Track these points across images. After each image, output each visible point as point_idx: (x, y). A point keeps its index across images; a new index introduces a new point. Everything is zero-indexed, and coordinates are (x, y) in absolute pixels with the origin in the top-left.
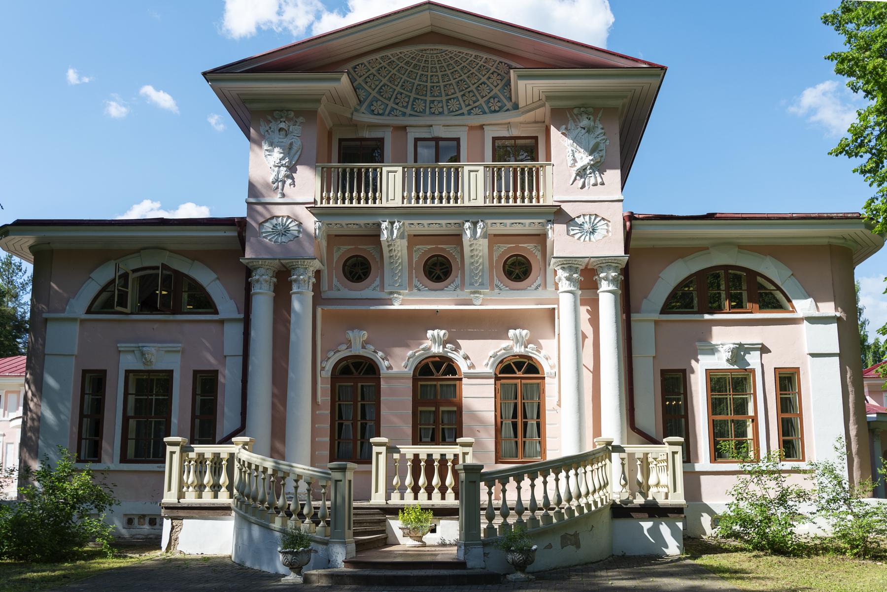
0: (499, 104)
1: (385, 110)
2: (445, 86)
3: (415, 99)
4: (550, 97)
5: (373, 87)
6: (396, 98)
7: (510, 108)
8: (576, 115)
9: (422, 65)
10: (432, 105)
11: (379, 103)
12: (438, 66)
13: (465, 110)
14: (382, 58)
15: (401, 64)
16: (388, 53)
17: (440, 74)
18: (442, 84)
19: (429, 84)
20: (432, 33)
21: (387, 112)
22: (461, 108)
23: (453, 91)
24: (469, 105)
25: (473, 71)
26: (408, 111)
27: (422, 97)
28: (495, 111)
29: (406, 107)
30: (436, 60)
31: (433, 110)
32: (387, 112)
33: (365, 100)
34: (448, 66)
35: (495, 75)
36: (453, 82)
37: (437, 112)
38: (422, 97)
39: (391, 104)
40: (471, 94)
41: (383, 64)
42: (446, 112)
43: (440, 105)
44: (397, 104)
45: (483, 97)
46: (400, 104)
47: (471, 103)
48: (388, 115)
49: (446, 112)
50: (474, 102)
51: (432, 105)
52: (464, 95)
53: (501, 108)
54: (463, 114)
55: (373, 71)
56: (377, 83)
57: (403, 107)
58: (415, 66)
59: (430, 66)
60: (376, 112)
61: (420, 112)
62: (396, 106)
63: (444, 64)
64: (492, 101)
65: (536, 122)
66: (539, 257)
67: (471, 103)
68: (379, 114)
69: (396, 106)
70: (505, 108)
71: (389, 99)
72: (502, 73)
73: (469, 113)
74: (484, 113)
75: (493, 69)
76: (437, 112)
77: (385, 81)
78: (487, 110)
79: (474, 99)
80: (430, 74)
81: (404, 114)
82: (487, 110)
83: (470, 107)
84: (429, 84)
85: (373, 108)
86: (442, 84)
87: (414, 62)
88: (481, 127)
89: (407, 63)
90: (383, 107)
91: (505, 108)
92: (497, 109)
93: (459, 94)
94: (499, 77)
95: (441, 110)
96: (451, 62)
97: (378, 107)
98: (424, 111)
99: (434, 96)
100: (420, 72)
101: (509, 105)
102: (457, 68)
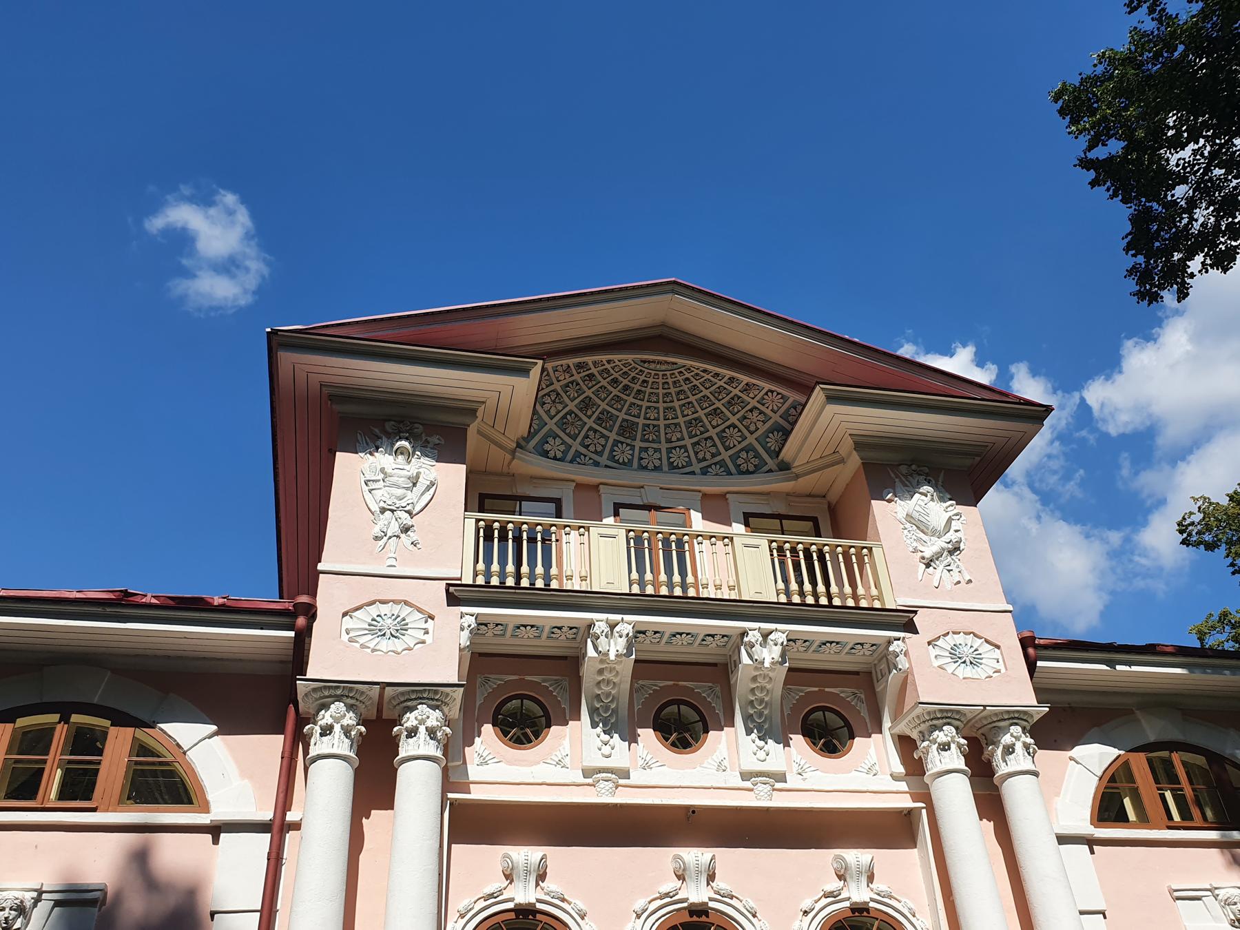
0: (756, 461)
1: (565, 453)
2: (667, 426)
3: (616, 443)
4: (863, 444)
5: (553, 412)
6: (587, 437)
7: (774, 467)
8: (905, 476)
9: (637, 387)
10: (644, 455)
11: (558, 441)
12: (661, 391)
13: (696, 467)
14: (580, 366)
15: (604, 383)
16: (589, 359)
17: (661, 406)
18: (662, 423)
19: (641, 421)
20: (660, 337)
21: (569, 457)
22: (689, 464)
23: (679, 435)
24: (704, 459)
25: (718, 404)
26: (603, 460)
27: (629, 441)
28: (748, 472)
29: (600, 454)
30: (661, 381)
31: (644, 463)
32: (569, 457)
33: (536, 432)
34: (678, 393)
35: (756, 413)
36: (681, 420)
37: (651, 466)
38: (629, 441)
39: (576, 446)
40: (709, 443)
41: (577, 377)
42: (665, 468)
43: (657, 455)
44: (587, 447)
45: (727, 449)
46: (592, 448)
47: (708, 456)
48: (571, 462)
49: (665, 468)
50: (713, 456)
51: (644, 455)
52: (697, 443)
53: (757, 469)
54: (693, 473)
55: (557, 386)
56: (560, 407)
57: (596, 452)
58: (626, 388)
59: (648, 390)
60: (551, 454)
61: (624, 463)
62: (583, 450)
63: (673, 390)
64: (744, 455)
65: (810, 496)
66: (864, 713)
67: (708, 456)
68: (555, 458)
69: (583, 450)
70: (766, 468)
71: (574, 438)
72: (768, 412)
73: (704, 472)
74: (730, 473)
75: (754, 403)
76: (651, 466)
77: (571, 406)
78: (733, 470)
79: (713, 450)
80: (645, 404)
81: (596, 464)
82: (733, 470)
83: (704, 464)
84: (641, 421)
85: (547, 447)
86: (662, 423)
87: (626, 382)
88: (723, 496)
89: (615, 381)
90: (562, 448)
91: (766, 468)
92: (751, 468)
93: (688, 442)
94: (761, 417)
95: (657, 463)
96: (685, 387)
97: (554, 447)
98: (630, 461)
99: (647, 441)
100: (631, 399)
101: (771, 463)
102: (692, 399)
